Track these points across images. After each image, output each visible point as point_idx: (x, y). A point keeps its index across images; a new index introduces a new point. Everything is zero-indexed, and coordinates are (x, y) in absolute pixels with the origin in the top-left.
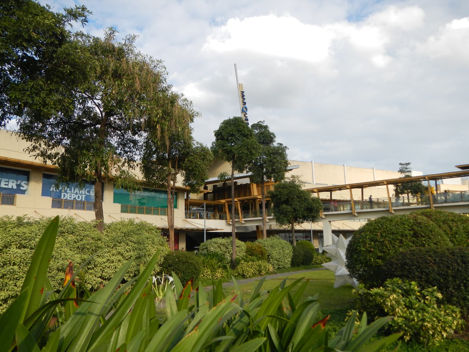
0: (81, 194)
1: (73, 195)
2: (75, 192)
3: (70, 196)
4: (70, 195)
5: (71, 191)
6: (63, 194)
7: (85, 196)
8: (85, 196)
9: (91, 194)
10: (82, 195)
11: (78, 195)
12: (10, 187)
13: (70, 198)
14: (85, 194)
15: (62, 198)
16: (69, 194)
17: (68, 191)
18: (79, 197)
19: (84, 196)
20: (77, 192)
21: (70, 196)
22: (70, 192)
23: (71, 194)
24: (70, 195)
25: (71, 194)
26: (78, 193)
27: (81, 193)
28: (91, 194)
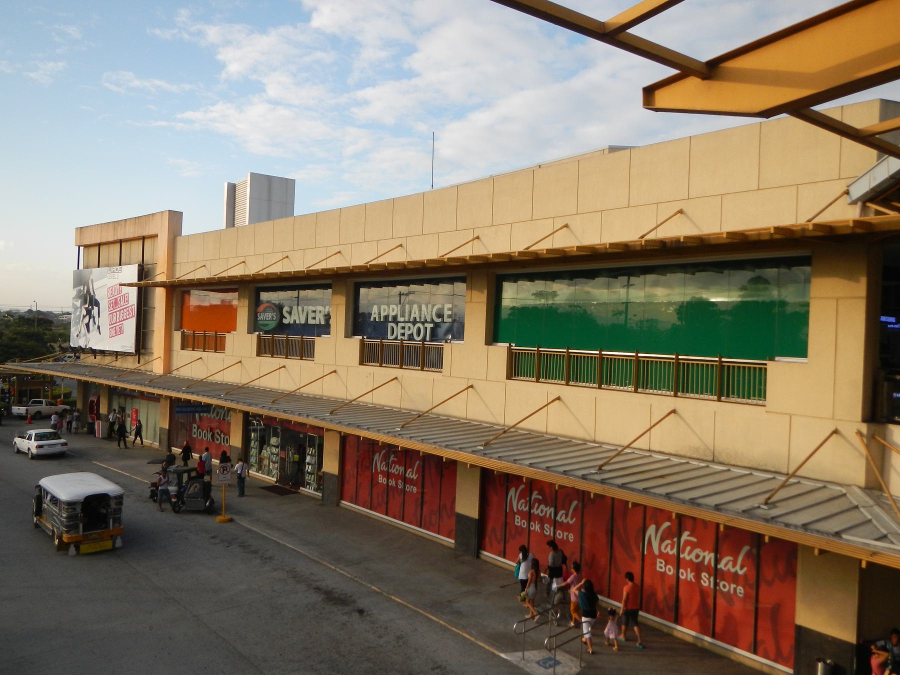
0: (423, 323)
2: (412, 320)
3: (403, 331)
6: (390, 325)
7: (432, 325)
10: (426, 325)
12: (318, 323)
15: (390, 337)
16: (400, 325)
18: (419, 330)
19: (429, 326)
20: (415, 318)
21: (403, 331)
23: (403, 325)
24: (403, 328)
25: (403, 325)
26: (418, 320)
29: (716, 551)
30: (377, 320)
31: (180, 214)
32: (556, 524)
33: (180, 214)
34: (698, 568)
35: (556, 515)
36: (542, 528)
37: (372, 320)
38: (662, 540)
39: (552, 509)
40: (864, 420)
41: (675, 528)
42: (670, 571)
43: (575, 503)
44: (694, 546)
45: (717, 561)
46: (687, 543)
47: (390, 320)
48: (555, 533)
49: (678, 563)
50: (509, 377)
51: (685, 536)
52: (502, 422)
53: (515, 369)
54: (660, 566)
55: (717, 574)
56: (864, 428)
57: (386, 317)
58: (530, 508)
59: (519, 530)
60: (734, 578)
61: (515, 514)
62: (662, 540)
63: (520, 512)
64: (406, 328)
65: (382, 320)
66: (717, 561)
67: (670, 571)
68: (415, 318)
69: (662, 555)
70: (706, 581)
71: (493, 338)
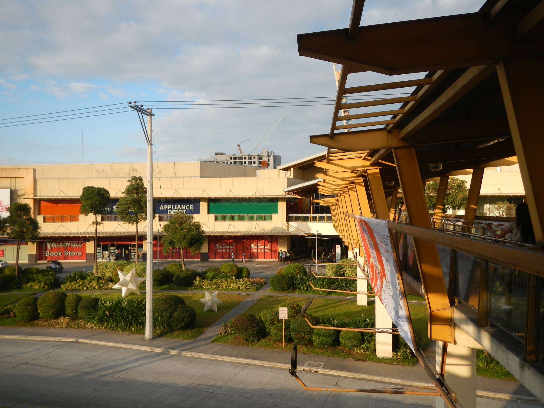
1: (176, 211)
2: (178, 209)
3: (174, 212)
4: (174, 211)
5: (175, 208)
6: (169, 211)
7: (186, 210)
8: (186, 210)
9: (191, 209)
10: (183, 210)
11: (180, 211)
13: (174, 213)
14: (186, 209)
16: (173, 211)
17: (172, 209)
19: (185, 211)
20: (179, 209)
21: (174, 212)
22: (174, 209)
23: (174, 210)
24: (174, 211)
25: (174, 210)
26: (180, 209)
27: (182, 209)
28: (191, 209)
29: (264, 245)
30: (163, 209)
31: (35, 169)
32: (229, 249)
33: (35, 169)
34: (261, 249)
35: (229, 247)
36: (226, 250)
37: (160, 209)
38: (254, 246)
39: (229, 246)
40: (287, 222)
41: (256, 244)
42: (256, 251)
43: (234, 244)
44: (260, 245)
45: (265, 247)
46: (259, 245)
47: (169, 209)
48: (229, 251)
49: (257, 249)
50: (215, 220)
51: (259, 244)
52: (214, 230)
53: (216, 219)
54: (254, 251)
55: (265, 249)
56: (287, 223)
57: (167, 209)
58: (222, 247)
59: (220, 252)
60: (268, 249)
61: (218, 249)
62: (254, 246)
63: (219, 249)
64: (176, 211)
65: (165, 209)
66: (265, 247)
67: (256, 251)
68: (179, 209)
69: (254, 249)
70: (263, 251)
71: (209, 213)
